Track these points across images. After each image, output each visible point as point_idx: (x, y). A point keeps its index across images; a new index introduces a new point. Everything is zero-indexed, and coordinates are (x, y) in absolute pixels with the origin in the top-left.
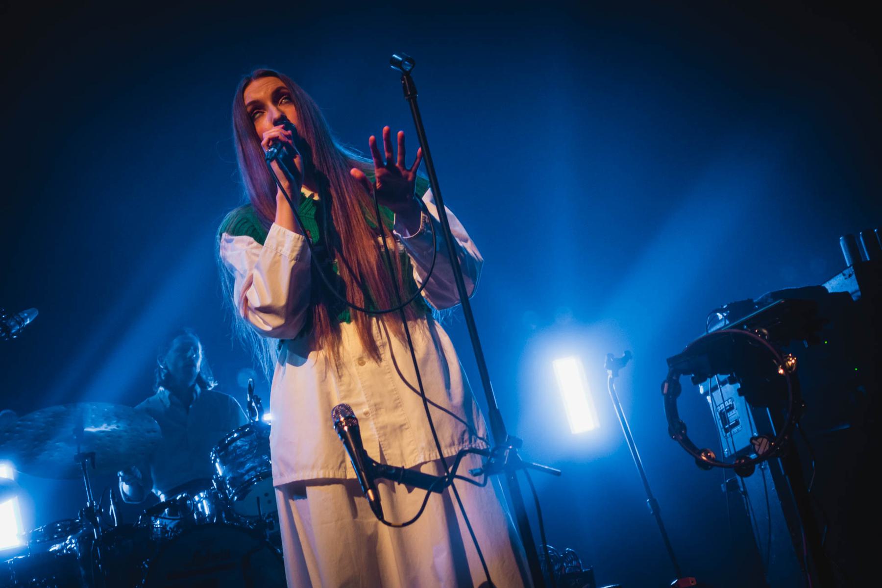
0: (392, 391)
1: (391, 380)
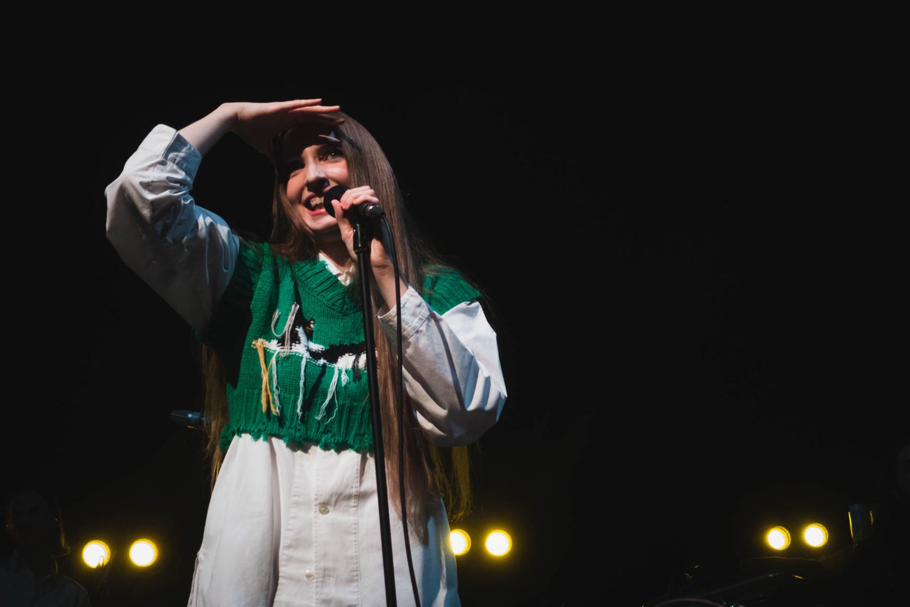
0: (352, 558)
1: (354, 543)
